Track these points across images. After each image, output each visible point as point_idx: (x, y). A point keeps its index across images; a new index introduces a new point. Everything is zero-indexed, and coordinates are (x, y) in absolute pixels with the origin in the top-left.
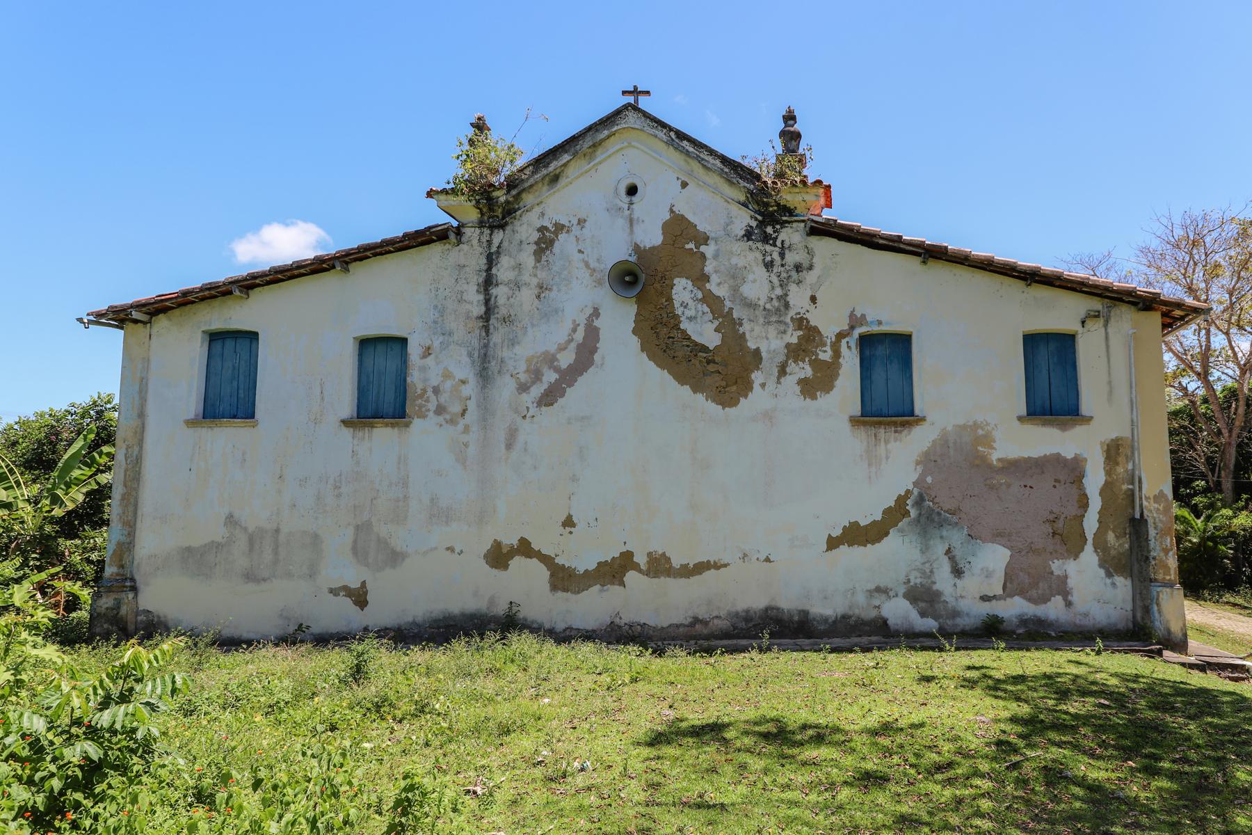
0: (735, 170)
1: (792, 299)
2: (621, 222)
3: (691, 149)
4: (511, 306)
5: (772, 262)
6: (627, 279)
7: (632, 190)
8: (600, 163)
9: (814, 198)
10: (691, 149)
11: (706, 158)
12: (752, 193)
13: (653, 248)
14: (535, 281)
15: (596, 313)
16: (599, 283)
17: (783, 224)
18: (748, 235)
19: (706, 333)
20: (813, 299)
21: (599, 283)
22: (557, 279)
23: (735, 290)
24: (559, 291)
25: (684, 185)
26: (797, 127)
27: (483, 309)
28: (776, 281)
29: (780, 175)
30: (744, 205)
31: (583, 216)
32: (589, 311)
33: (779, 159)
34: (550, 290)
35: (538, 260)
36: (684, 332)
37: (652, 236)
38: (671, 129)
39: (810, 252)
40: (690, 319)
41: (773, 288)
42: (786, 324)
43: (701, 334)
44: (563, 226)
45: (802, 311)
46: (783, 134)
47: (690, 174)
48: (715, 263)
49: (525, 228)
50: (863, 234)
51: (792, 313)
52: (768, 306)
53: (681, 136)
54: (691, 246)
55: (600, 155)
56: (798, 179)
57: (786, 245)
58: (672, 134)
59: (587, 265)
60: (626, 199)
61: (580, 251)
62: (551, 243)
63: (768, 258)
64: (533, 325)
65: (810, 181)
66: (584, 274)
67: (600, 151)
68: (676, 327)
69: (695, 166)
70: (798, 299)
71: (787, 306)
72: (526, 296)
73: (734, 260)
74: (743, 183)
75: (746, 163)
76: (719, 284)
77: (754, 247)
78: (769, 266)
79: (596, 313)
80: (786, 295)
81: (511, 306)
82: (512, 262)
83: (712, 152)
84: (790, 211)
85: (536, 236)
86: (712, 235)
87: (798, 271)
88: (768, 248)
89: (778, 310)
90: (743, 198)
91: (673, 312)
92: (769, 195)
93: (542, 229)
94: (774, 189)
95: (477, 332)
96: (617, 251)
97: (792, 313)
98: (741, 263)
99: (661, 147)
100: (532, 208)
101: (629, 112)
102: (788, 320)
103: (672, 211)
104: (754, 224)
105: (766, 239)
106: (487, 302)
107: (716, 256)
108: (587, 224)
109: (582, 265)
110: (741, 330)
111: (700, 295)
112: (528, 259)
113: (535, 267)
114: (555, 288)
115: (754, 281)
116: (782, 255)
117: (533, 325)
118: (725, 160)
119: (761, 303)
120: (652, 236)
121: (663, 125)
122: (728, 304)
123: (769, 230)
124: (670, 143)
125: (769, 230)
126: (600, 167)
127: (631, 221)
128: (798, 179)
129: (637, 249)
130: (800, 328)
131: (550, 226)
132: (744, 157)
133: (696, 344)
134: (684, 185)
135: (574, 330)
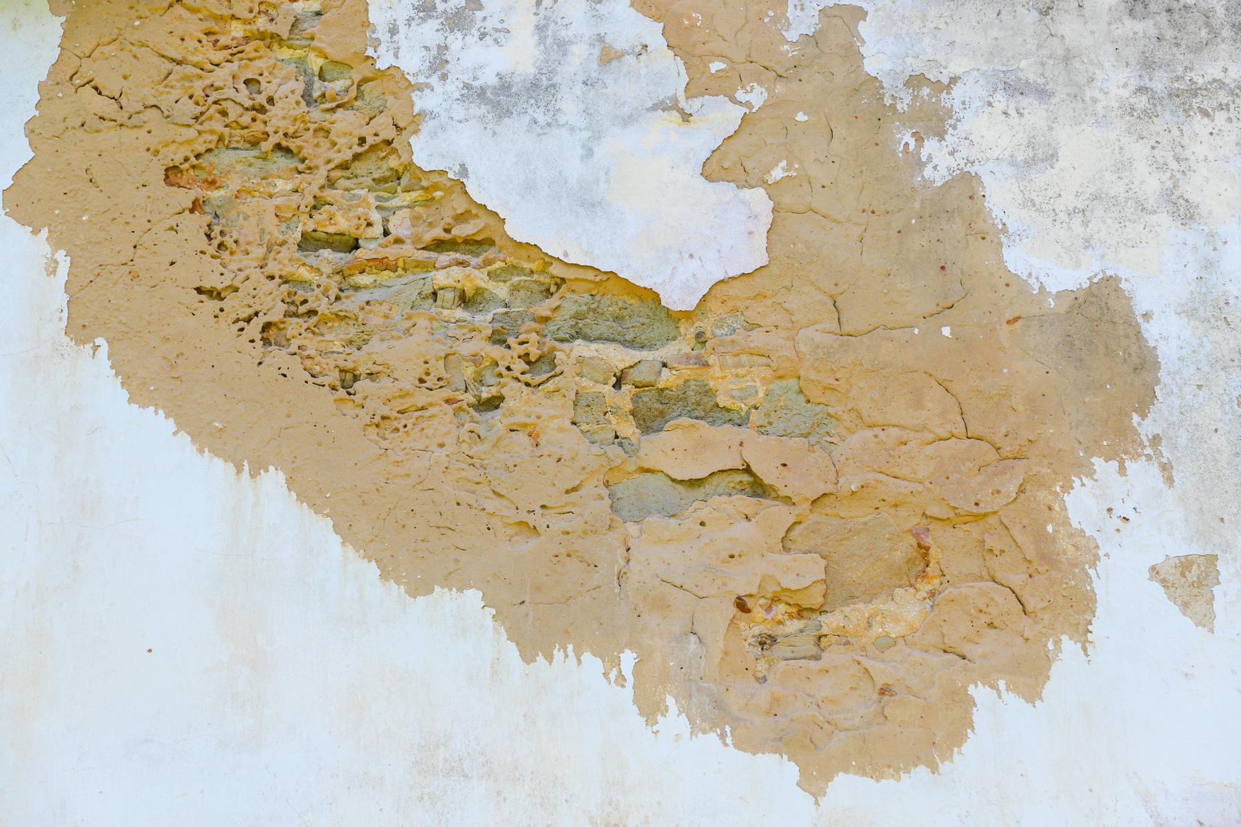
19: (644, 199)
40: (498, 99)
68: (381, 157)
110: (939, 161)
133: (552, 278)
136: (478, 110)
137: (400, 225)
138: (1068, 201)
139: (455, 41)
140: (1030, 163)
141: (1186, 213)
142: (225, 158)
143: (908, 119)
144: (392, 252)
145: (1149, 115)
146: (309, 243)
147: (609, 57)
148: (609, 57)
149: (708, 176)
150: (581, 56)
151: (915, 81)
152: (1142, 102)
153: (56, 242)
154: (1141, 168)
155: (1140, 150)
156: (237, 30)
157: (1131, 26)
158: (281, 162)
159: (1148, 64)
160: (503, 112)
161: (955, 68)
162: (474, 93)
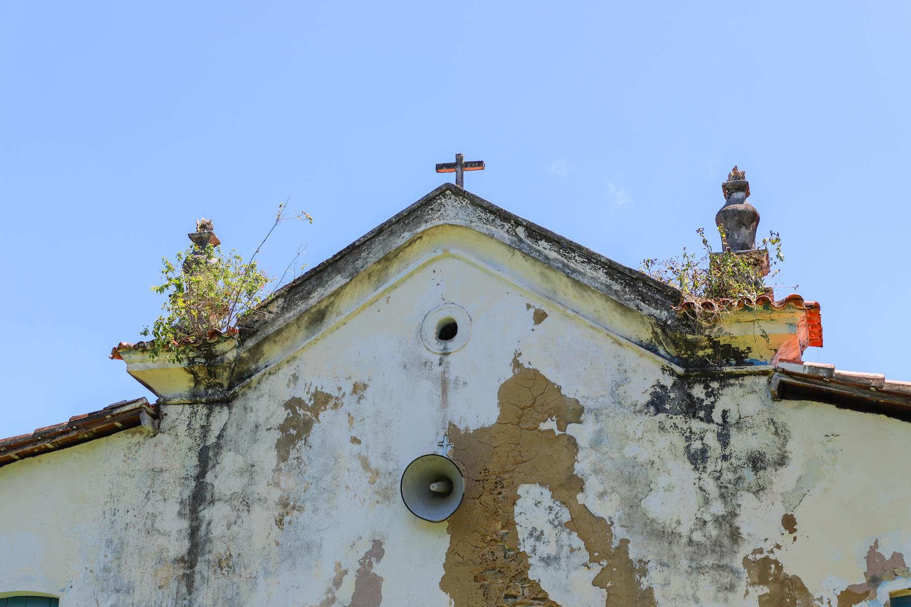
0: (632, 285)
1: (744, 523)
2: (428, 387)
3: (553, 255)
4: (233, 538)
6: (434, 487)
7: (448, 331)
8: (395, 287)
9: (783, 330)
10: (553, 255)
11: (580, 268)
12: (664, 326)
13: (482, 431)
14: (275, 494)
15: (377, 550)
16: (385, 495)
17: (724, 380)
18: (658, 402)
20: (789, 523)
21: (385, 495)
22: (312, 489)
23: (633, 505)
24: (315, 510)
25: (540, 317)
26: (752, 202)
27: (186, 544)
28: (712, 488)
29: (719, 292)
30: (651, 348)
31: (361, 378)
32: (365, 547)
33: (717, 263)
34: (300, 509)
35: (283, 458)
36: (535, 585)
37: (479, 409)
38: (518, 222)
39: (779, 431)
40: (547, 561)
41: (707, 501)
42: (733, 571)
43: (567, 591)
44: (328, 397)
45: (767, 547)
46: (723, 217)
47: (551, 297)
48: (594, 456)
49: (265, 403)
50: (889, 393)
51: (745, 550)
52: (697, 536)
53: (536, 233)
54: (550, 425)
55: (396, 272)
56: (753, 297)
57: (732, 418)
58: (521, 231)
59: (365, 464)
60: (437, 346)
61: (355, 440)
62: (305, 427)
63: (697, 445)
64: (267, 573)
65: (779, 296)
66: (359, 480)
67: (395, 266)
68: (521, 575)
69: (560, 282)
70: (758, 522)
71: (735, 536)
72: (260, 519)
73: (630, 450)
74: (646, 309)
75: (653, 272)
76: (602, 495)
77: (668, 423)
78: (698, 458)
79: (377, 550)
80: (733, 515)
81: (233, 538)
82: (240, 462)
83: (590, 258)
84: (739, 356)
85: (281, 415)
86: (588, 404)
87: (755, 468)
88: (696, 425)
89: (717, 544)
90: (646, 335)
91: (514, 548)
92: (695, 328)
93: (293, 404)
94: (706, 317)
95: (174, 585)
96: (417, 436)
97: (745, 550)
98: (644, 455)
99: (501, 254)
100: (279, 368)
101: (451, 193)
102: (738, 563)
103: (516, 364)
104: (668, 381)
105: (692, 408)
106: (194, 532)
107: (596, 443)
108: (368, 393)
109: (357, 464)
110: (645, 583)
111: (566, 516)
112: (265, 454)
113: (278, 470)
114: (308, 505)
115: (669, 489)
116: (724, 439)
117: (267, 573)
118: (613, 270)
119: (684, 530)
120: (479, 409)
121: (504, 216)
122: (619, 532)
123: (698, 391)
124: (516, 246)
125: (698, 391)
126: (393, 294)
127: (445, 385)
128: (753, 297)
129: (453, 433)
130: (762, 581)
131: (306, 398)
132: (649, 263)
134: (540, 317)
135: (338, 583)
136: (543, 564)
137: (526, 594)
138: (672, 596)
139: (538, 544)
140: (664, 585)
141: (697, 601)
142: (488, 573)
143: (638, 571)
144: (524, 601)
145: (691, 573)
146: (507, 597)
147: (572, 550)
148: (572, 550)
149: (594, 585)
150: (566, 550)
151: (640, 561)
152: (689, 570)
153: (451, 597)
154: (688, 588)
155: (688, 583)
156: (489, 538)
157: (689, 549)
158: (500, 575)
159: (692, 560)
160: (548, 565)
161: (649, 558)
162: (542, 559)
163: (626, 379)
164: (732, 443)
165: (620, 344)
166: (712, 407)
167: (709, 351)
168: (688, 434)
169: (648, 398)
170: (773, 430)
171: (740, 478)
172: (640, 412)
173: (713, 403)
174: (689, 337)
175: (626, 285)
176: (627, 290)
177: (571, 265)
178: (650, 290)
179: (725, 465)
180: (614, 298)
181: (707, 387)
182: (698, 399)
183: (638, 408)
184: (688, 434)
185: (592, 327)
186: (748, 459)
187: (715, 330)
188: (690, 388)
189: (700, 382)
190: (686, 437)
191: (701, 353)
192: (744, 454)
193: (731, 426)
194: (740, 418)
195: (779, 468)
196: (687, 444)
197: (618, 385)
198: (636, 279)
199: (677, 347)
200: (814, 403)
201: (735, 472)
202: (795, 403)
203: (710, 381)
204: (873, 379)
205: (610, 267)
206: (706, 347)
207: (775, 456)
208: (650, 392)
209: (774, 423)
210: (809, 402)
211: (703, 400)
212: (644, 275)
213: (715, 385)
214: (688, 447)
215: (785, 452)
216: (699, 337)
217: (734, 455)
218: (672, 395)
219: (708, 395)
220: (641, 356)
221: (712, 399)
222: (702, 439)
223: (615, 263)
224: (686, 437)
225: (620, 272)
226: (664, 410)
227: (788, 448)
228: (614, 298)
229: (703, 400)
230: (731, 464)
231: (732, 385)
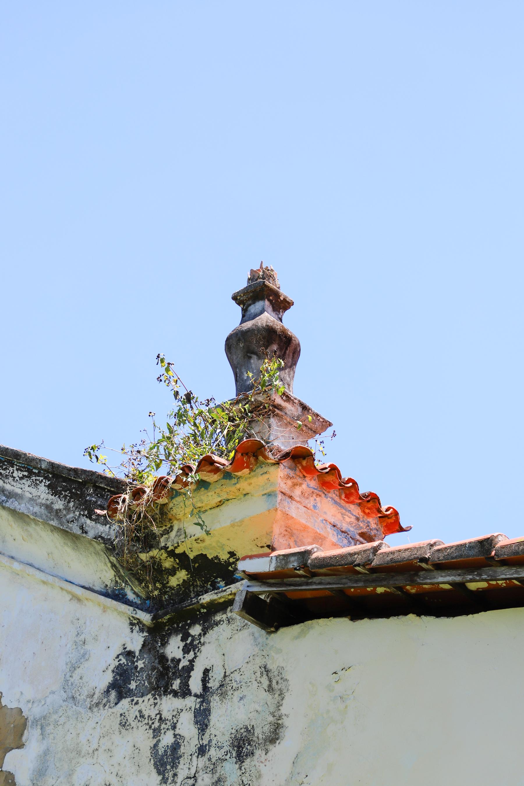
5: (175, 747)
63: (167, 739)
86: (31, 712)
88: (169, 704)
104: (136, 641)
105: (166, 678)
125: (174, 648)
132: (91, 452)
163: (84, 655)
164: (212, 723)
165: (79, 600)
166: (190, 668)
167: (182, 575)
168: (157, 724)
169: (109, 678)
170: (265, 682)
171: (219, 780)
172: (97, 704)
173: (192, 661)
174: (144, 557)
175: (71, 497)
176: (71, 504)
177: (8, 487)
178: (102, 496)
179: (202, 762)
180: (54, 523)
181: (185, 636)
182: (173, 660)
183: (95, 700)
184: (157, 724)
185: (44, 583)
186: (233, 745)
187: (173, 534)
188: (164, 644)
189: (176, 631)
190: (154, 730)
191: (174, 581)
192: (227, 737)
193: (213, 693)
194: (225, 676)
195: (271, 747)
196: (155, 741)
197: (74, 668)
198: (84, 484)
199: (140, 581)
200: (322, 621)
201: (213, 771)
202: (296, 629)
203: (190, 626)
204: (355, 554)
205: (55, 476)
206: (173, 572)
207: (267, 729)
208: (112, 667)
209: (267, 671)
210: (315, 621)
211: (179, 660)
212: (93, 473)
213: (196, 630)
214: (156, 745)
215: (280, 717)
216: (154, 552)
217: (214, 742)
218: (140, 664)
219: (186, 650)
220: (105, 609)
221: (191, 655)
222: (174, 727)
223: (59, 466)
224: (154, 730)
225: (66, 480)
226: (129, 693)
227: (284, 710)
228: (54, 523)
229: (179, 660)
230: (210, 759)
231: (217, 624)
